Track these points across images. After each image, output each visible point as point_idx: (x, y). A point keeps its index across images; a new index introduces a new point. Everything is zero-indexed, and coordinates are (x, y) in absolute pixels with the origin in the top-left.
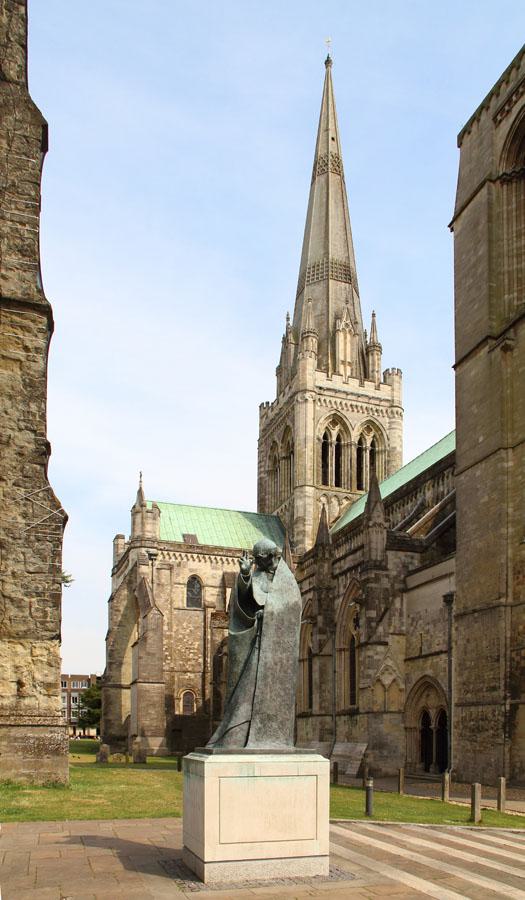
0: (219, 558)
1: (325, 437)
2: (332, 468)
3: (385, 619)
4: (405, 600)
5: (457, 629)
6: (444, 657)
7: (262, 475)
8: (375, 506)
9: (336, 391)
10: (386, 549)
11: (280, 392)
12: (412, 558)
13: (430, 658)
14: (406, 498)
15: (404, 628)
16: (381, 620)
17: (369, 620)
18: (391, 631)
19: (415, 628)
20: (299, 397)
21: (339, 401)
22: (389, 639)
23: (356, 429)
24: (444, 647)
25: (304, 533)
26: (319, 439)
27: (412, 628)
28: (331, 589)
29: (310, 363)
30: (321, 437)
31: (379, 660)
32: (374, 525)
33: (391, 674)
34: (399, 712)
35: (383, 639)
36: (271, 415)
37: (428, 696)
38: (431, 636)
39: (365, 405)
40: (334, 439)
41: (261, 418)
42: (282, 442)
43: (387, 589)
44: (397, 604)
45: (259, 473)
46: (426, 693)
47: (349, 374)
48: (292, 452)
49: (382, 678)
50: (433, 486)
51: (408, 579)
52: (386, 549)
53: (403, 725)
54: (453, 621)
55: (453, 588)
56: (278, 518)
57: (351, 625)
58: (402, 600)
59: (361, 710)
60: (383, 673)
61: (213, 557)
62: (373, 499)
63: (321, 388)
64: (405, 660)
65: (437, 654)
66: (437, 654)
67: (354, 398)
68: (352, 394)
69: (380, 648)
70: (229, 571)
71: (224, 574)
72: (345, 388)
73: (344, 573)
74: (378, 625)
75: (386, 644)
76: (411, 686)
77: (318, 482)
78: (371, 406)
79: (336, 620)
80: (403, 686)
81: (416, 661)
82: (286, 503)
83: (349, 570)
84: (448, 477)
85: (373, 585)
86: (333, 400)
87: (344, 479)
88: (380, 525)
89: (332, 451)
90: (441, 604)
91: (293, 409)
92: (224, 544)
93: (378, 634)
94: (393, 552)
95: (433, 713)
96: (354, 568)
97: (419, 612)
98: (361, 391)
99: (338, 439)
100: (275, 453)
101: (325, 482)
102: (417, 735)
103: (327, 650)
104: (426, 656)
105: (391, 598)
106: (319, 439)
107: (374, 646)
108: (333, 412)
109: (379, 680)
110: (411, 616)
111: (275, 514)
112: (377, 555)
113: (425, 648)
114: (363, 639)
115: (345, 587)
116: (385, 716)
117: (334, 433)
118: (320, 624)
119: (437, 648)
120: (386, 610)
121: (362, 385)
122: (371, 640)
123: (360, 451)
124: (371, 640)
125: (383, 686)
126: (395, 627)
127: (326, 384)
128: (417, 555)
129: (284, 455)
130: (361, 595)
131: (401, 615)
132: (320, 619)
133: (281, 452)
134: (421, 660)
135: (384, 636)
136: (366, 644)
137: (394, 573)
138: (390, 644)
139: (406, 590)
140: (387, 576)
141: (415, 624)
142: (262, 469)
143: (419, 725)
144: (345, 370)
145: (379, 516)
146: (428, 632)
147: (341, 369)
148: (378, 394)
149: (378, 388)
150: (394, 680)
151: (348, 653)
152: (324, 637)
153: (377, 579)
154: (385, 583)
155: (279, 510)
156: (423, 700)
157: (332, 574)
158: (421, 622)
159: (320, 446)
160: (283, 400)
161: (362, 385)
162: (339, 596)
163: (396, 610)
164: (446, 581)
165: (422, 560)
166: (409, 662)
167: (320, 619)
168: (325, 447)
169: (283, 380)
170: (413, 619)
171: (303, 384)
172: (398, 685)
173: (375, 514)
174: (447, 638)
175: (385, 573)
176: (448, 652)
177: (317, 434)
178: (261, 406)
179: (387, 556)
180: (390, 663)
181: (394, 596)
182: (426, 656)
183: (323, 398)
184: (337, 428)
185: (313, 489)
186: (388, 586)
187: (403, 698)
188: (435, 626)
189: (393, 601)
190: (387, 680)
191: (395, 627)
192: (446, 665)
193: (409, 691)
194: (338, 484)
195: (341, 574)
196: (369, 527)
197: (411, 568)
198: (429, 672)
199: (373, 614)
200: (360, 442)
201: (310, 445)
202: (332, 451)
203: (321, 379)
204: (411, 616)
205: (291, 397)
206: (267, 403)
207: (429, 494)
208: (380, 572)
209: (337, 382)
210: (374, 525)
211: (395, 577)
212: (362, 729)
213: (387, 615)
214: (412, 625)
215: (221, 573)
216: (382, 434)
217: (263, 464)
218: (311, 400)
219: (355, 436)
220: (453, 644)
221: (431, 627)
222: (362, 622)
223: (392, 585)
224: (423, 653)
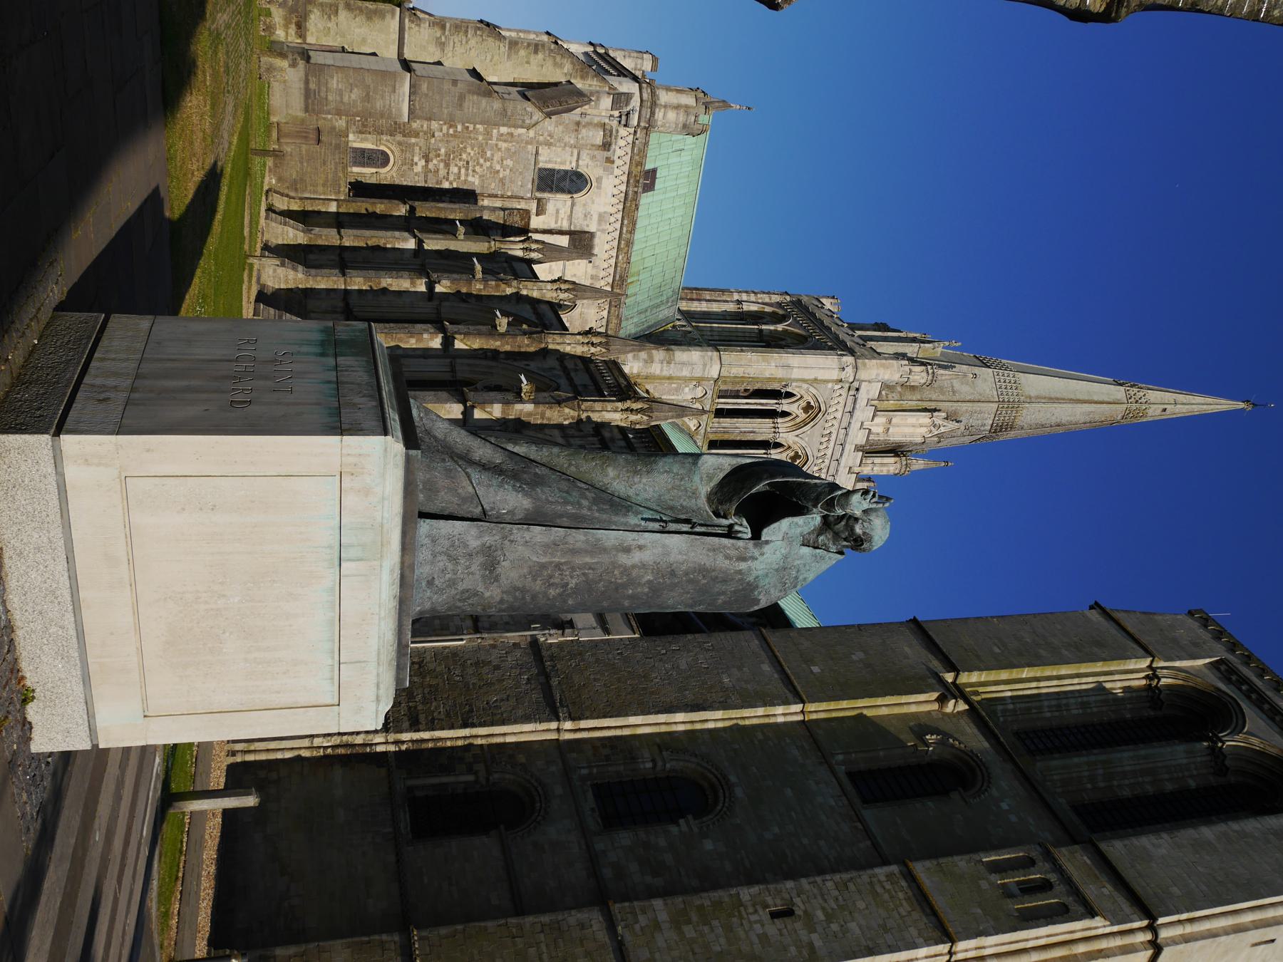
0: (618, 225)
1: (789, 395)
2: (743, 404)
9: (851, 413)
23: (797, 439)
25: (650, 360)
26: (785, 386)
39: (829, 452)
40: (786, 408)
47: (874, 430)
61: (619, 216)
63: (857, 390)
67: (841, 436)
68: (846, 435)
70: (597, 241)
71: (592, 235)
72: (855, 425)
77: (725, 382)
78: (827, 462)
86: (840, 407)
87: (727, 422)
89: (769, 404)
91: (831, 348)
92: (638, 235)
98: (849, 447)
99: (785, 414)
106: (785, 386)
108: (823, 408)
117: (794, 408)
121: (858, 448)
127: (863, 397)
144: (877, 425)
147: (880, 419)
159: (776, 386)
161: (858, 448)
168: (775, 395)
171: (865, 365)
177: (794, 384)
183: (844, 392)
184: (803, 416)
185: (716, 377)
194: (720, 413)
200: (777, 445)
201: (780, 373)
202: (769, 404)
203: (870, 391)
209: (864, 413)
215: (592, 229)
218: (843, 375)
219: (786, 437)
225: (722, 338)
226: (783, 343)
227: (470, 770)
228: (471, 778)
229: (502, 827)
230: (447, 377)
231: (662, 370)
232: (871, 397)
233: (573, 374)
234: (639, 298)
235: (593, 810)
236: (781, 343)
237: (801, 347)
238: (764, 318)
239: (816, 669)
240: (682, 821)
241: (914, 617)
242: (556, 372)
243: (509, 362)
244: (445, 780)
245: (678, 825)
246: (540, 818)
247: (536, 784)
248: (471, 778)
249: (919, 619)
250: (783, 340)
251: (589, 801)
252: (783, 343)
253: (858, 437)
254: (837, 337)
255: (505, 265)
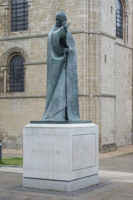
227: (3, 72)
228: (5, 72)
229: (24, 64)
235: (21, 33)
240: (29, 4)
244: (5, 80)
245: (30, 5)
246: (22, 51)
247: (10, 51)
248: (5, 72)
251: (18, 34)
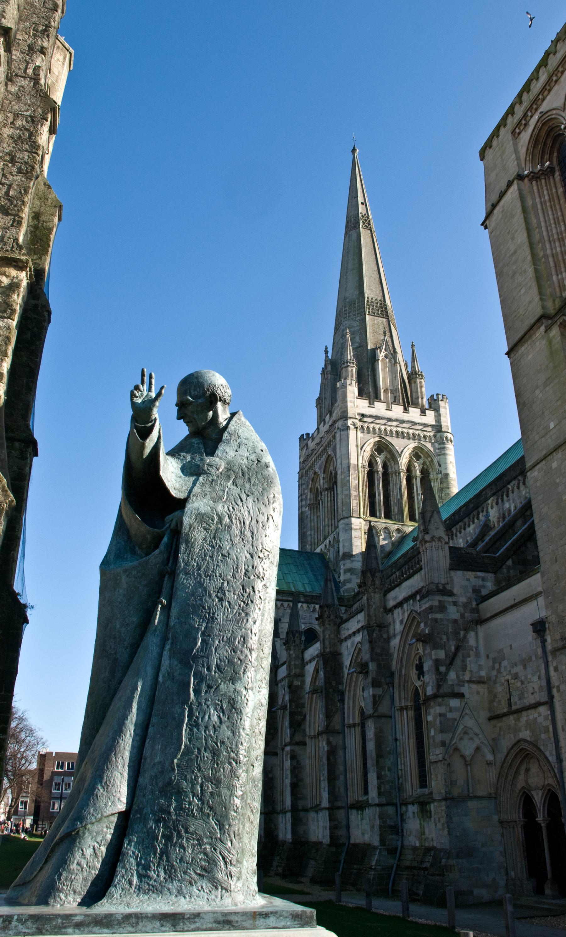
2: (380, 497)
3: (458, 662)
4: (481, 634)
5: (556, 669)
6: (543, 710)
7: (304, 509)
8: (431, 517)
10: (450, 569)
11: (321, 419)
12: (483, 579)
13: (524, 713)
14: (466, 520)
15: (483, 673)
16: (451, 663)
17: (437, 663)
18: (467, 678)
19: (499, 671)
20: (339, 424)
21: (383, 427)
22: (465, 690)
24: (544, 698)
27: (494, 673)
28: (385, 627)
29: (352, 390)
30: (366, 465)
31: (455, 719)
32: (433, 538)
33: (471, 739)
34: (489, 797)
35: (456, 690)
36: (311, 445)
37: (528, 770)
38: (522, 683)
41: (301, 449)
42: (324, 473)
43: (455, 621)
44: (472, 642)
45: (300, 507)
46: (523, 768)
48: (336, 483)
49: (461, 747)
50: (497, 503)
51: (481, 606)
52: (450, 569)
53: (496, 818)
54: (550, 658)
55: (543, 614)
56: (321, 556)
57: (414, 673)
58: (477, 634)
59: (436, 796)
60: (461, 739)
62: (429, 508)
64: (490, 719)
65: (535, 706)
66: (535, 706)
69: (454, 703)
72: (389, 414)
73: (400, 605)
74: (448, 670)
75: (461, 696)
76: (501, 756)
79: (394, 668)
80: (490, 757)
81: (505, 719)
82: (331, 538)
83: (406, 600)
84: (513, 493)
85: (438, 616)
88: (440, 539)
90: (530, 636)
91: (334, 437)
93: (450, 683)
94: (460, 573)
95: (538, 797)
96: (412, 597)
97: (501, 651)
98: (406, 417)
99: (385, 466)
100: (317, 485)
101: (373, 513)
102: (519, 833)
103: (384, 708)
104: (519, 711)
105: (462, 633)
107: (446, 699)
109: (456, 749)
110: (492, 656)
111: (318, 550)
112: (440, 578)
113: (514, 699)
114: (430, 691)
115: (401, 622)
116: (471, 804)
118: (372, 675)
119: (532, 700)
120: (458, 648)
121: (406, 410)
122: (441, 691)
123: (409, 479)
124: (441, 691)
125: (463, 757)
126: (471, 671)
128: (490, 576)
129: (326, 486)
130: (423, 630)
131: (477, 655)
132: (372, 666)
133: (322, 482)
134: (512, 717)
135: (459, 685)
136: (435, 696)
137: (463, 599)
138: (467, 695)
139: (481, 621)
140: (455, 604)
141: (497, 666)
142: (304, 503)
143: (517, 816)
145: (437, 529)
146: (516, 676)
148: (424, 420)
149: (423, 412)
150: (478, 749)
151: (411, 713)
152: (379, 691)
153: (442, 608)
154: (453, 613)
155: (322, 547)
156: (522, 777)
157: (385, 608)
158: (505, 663)
160: (324, 429)
162: (395, 636)
163: (471, 648)
164: (534, 604)
165: (497, 582)
166: (494, 722)
167: (372, 666)
168: (371, 475)
169: (324, 411)
170: (494, 660)
172: (483, 756)
173: (432, 527)
174: (544, 683)
175: (450, 599)
176: (550, 703)
178: (301, 438)
179: (451, 577)
180: (469, 722)
181: (466, 630)
182: (519, 711)
183: (366, 425)
186: (456, 616)
187: (492, 774)
188: (525, 667)
189: (465, 637)
190: (468, 748)
191: (471, 671)
192: (548, 723)
193: (498, 765)
195: (396, 607)
196: (426, 542)
197: (484, 592)
198: (526, 734)
199: (441, 654)
204: (492, 656)
205: (331, 426)
206: (308, 434)
207: (493, 514)
208: (446, 598)
210: (433, 538)
211: (465, 605)
212: (439, 826)
213: (460, 655)
214: (493, 668)
216: (432, 461)
217: (304, 497)
220: (555, 691)
221: (519, 669)
222: (427, 666)
223: (463, 616)
224: (514, 708)
225: (333, 517)
226: (333, 472)
230: (358, 730)
231: (359, 561)
232: (368, 405)
233: (350, 632)
234: (306, 581)
236: (333, 474)
237: (334, 459)
238: (317, 488)
239: (552, 425)
241: (506, 354)
242: (349, 647)
243: (345, 681)
249: (506, 350)
250: (331, 473)
252: (333, 472)
253: (397, 411)
254: (327, 432)
255: (280, 685)
